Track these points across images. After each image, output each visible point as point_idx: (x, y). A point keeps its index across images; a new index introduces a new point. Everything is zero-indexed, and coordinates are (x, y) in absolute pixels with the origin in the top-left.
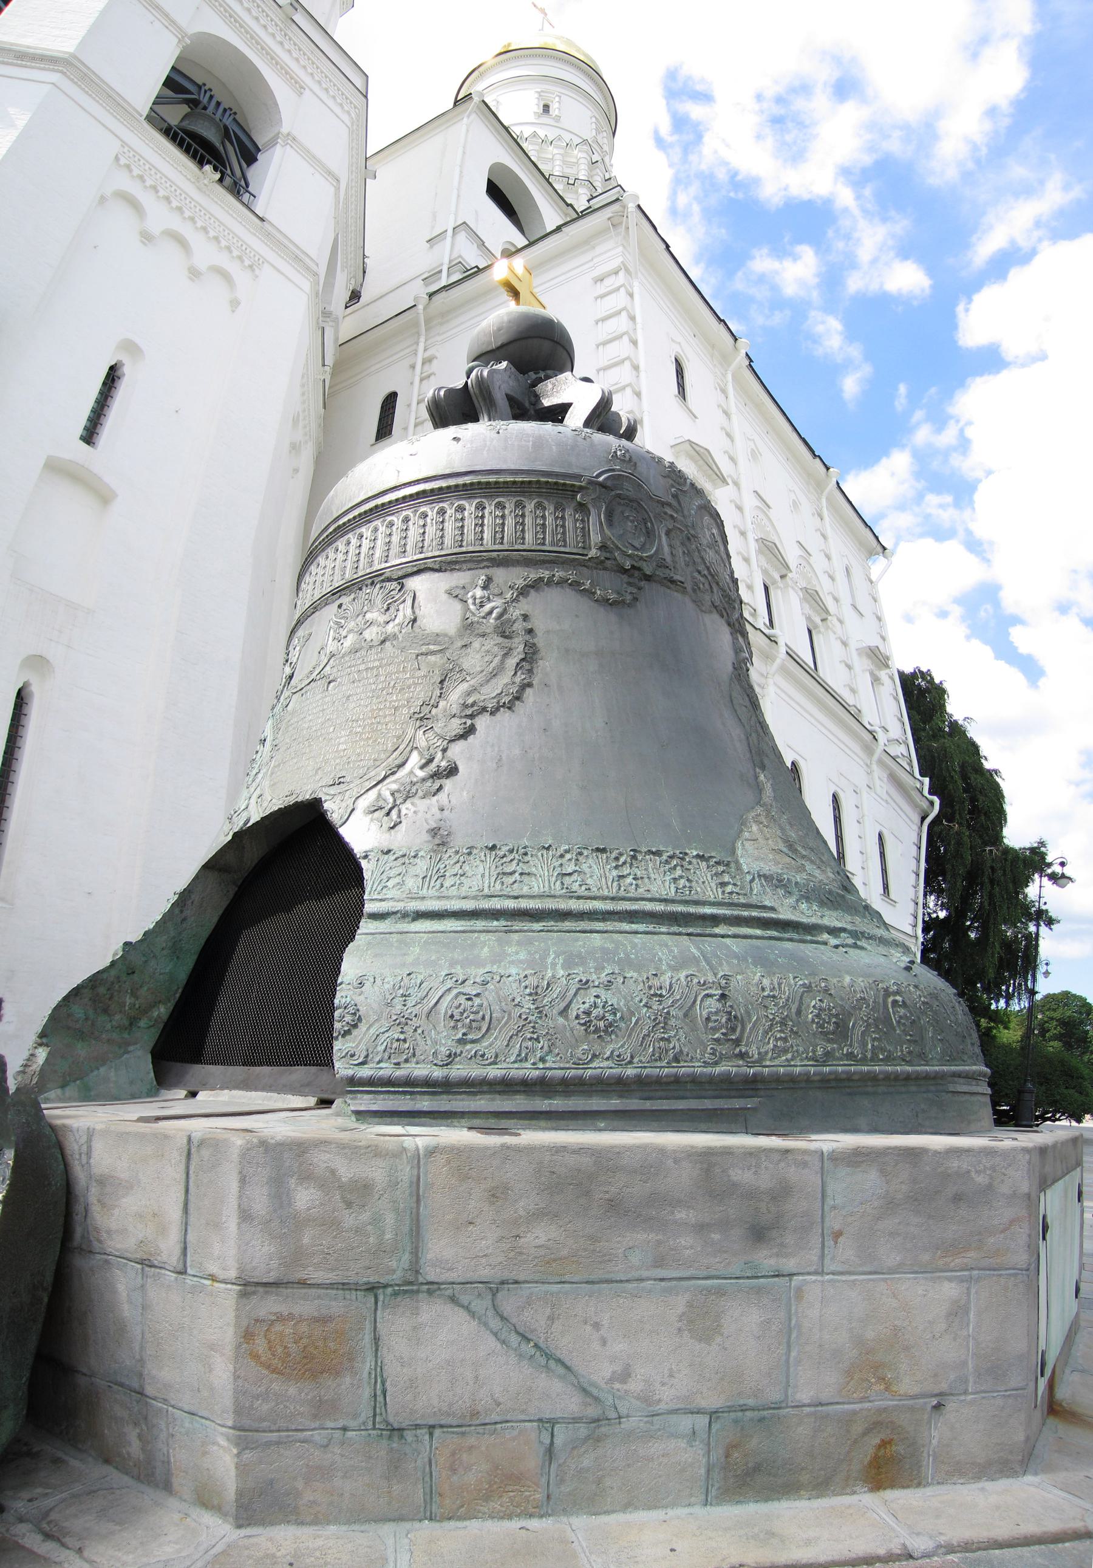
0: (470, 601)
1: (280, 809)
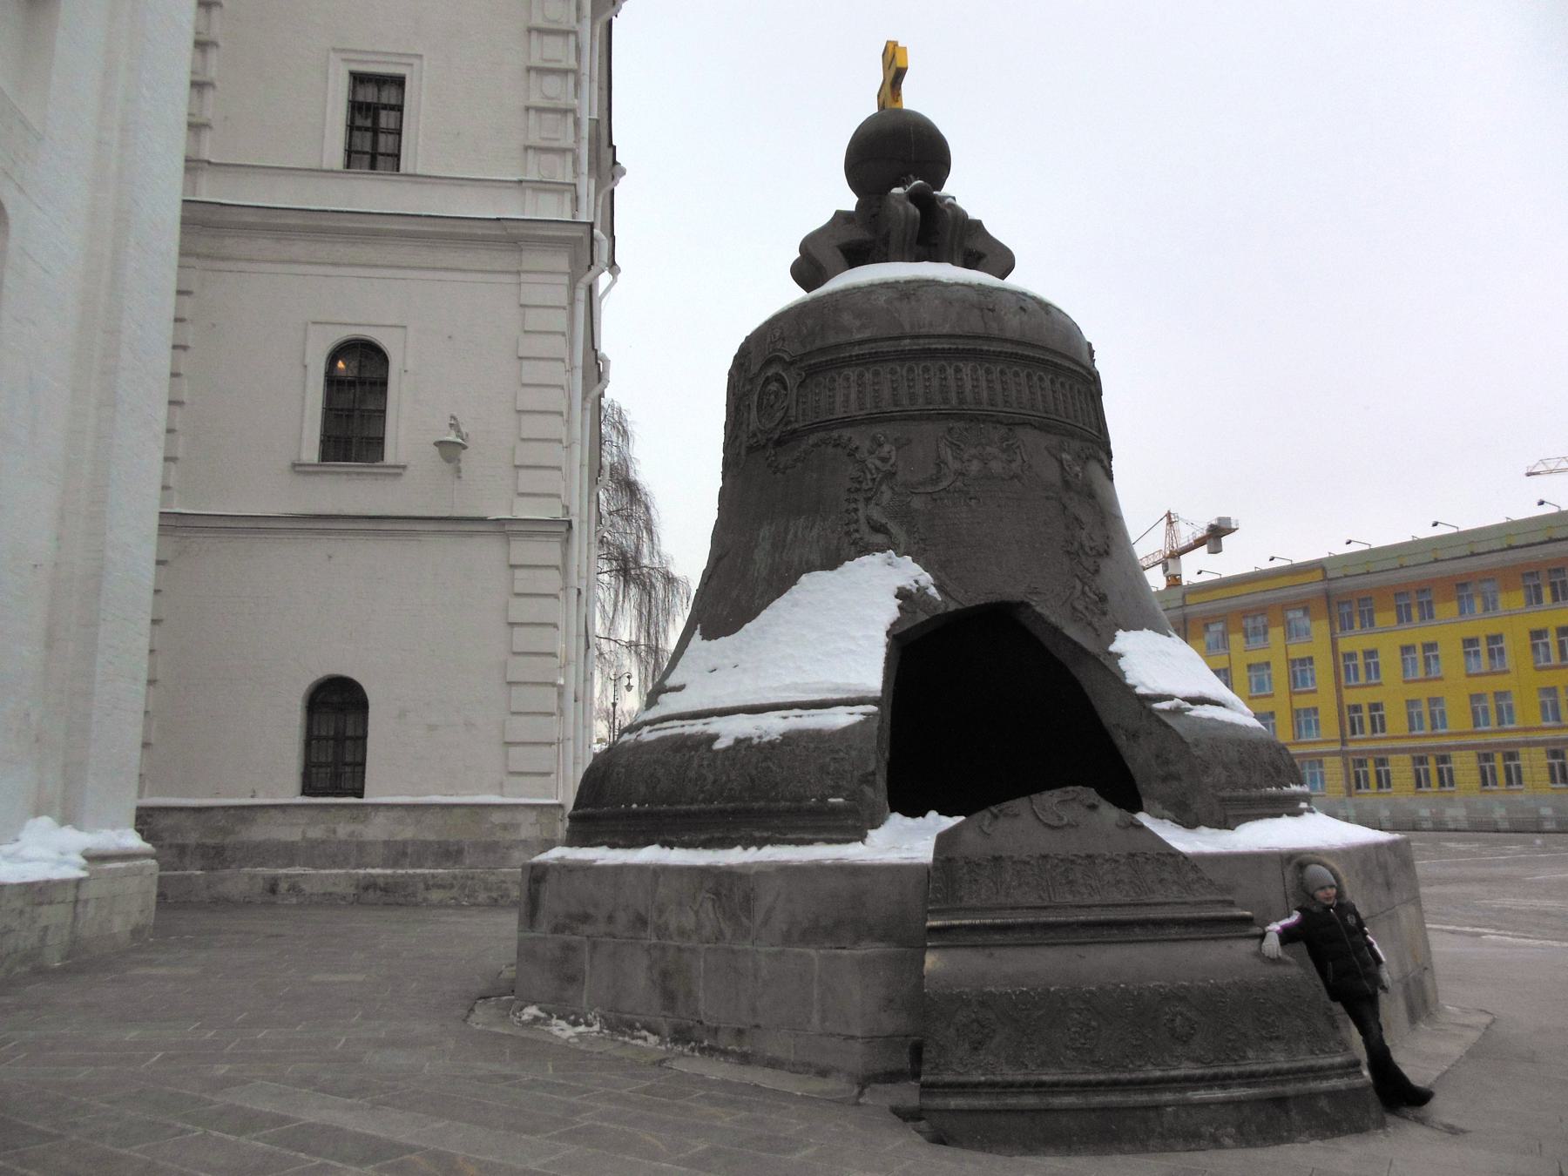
0: (1064, 462)
1: (986, 604)
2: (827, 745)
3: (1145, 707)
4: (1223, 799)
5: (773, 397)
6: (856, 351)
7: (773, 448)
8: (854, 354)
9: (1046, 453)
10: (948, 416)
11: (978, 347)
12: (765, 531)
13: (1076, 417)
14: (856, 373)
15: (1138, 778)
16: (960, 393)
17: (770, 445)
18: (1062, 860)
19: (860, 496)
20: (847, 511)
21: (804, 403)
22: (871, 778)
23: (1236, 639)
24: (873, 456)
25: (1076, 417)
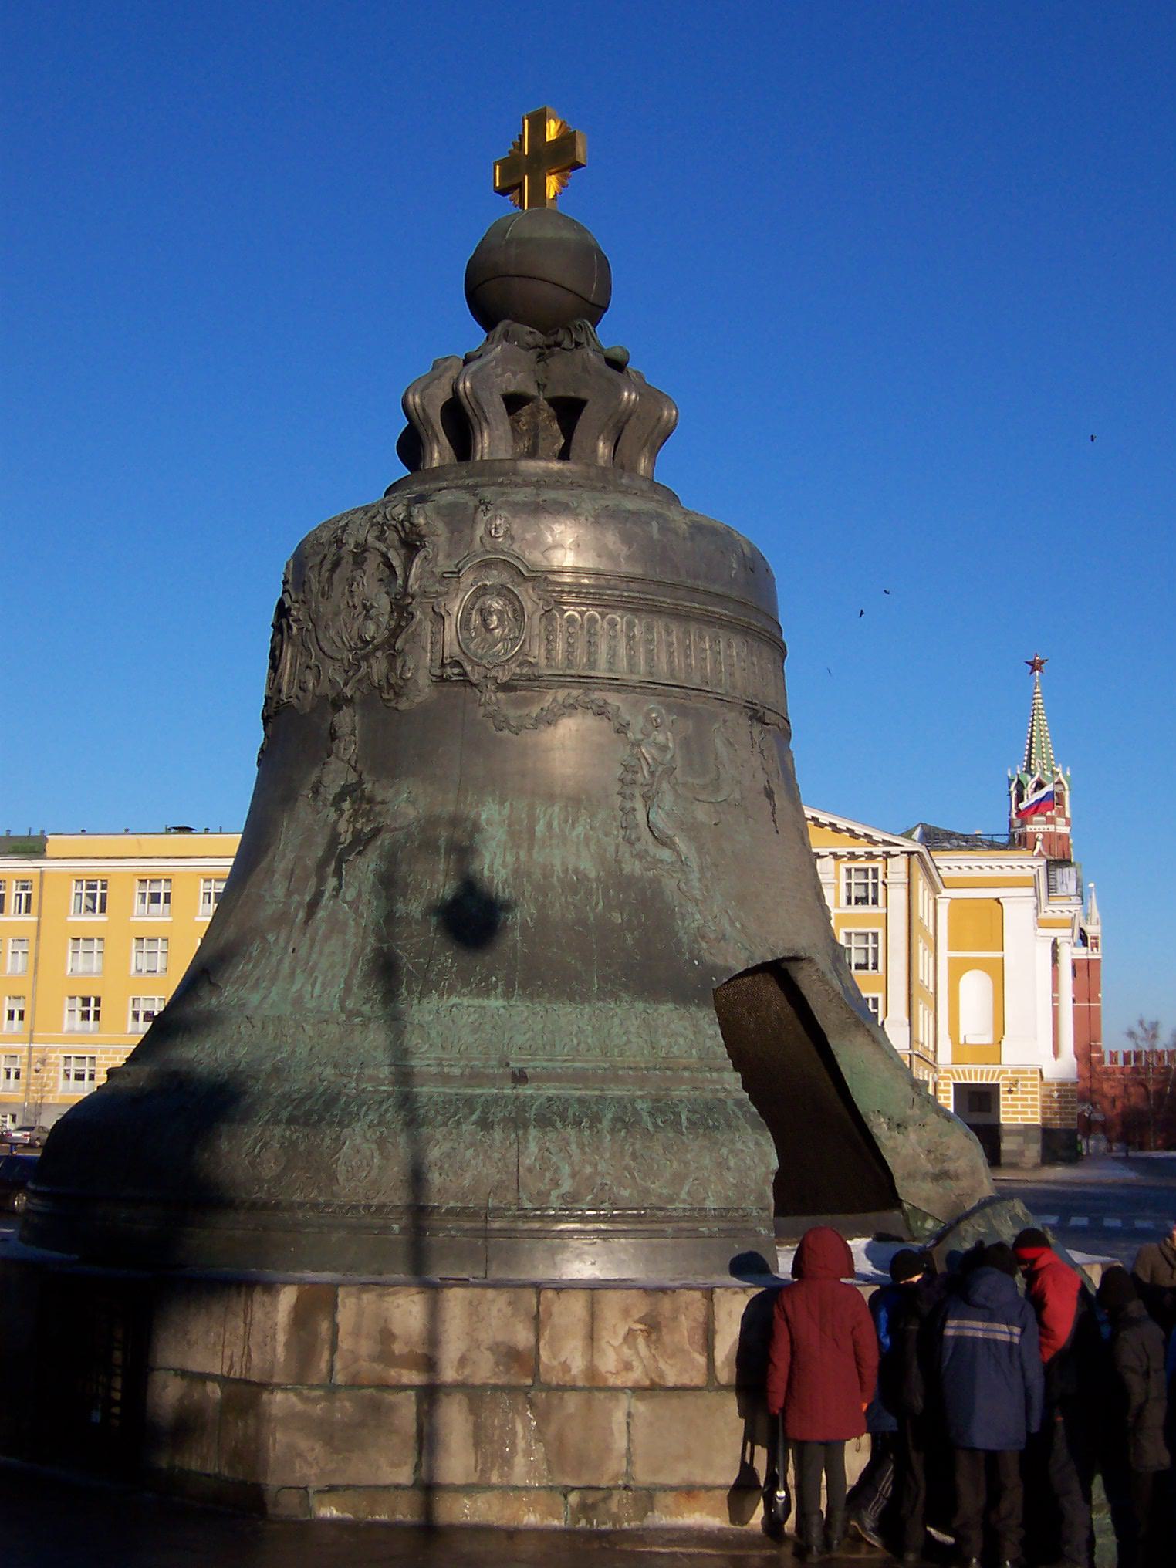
15: (897, 1175)
19: (637, 792)
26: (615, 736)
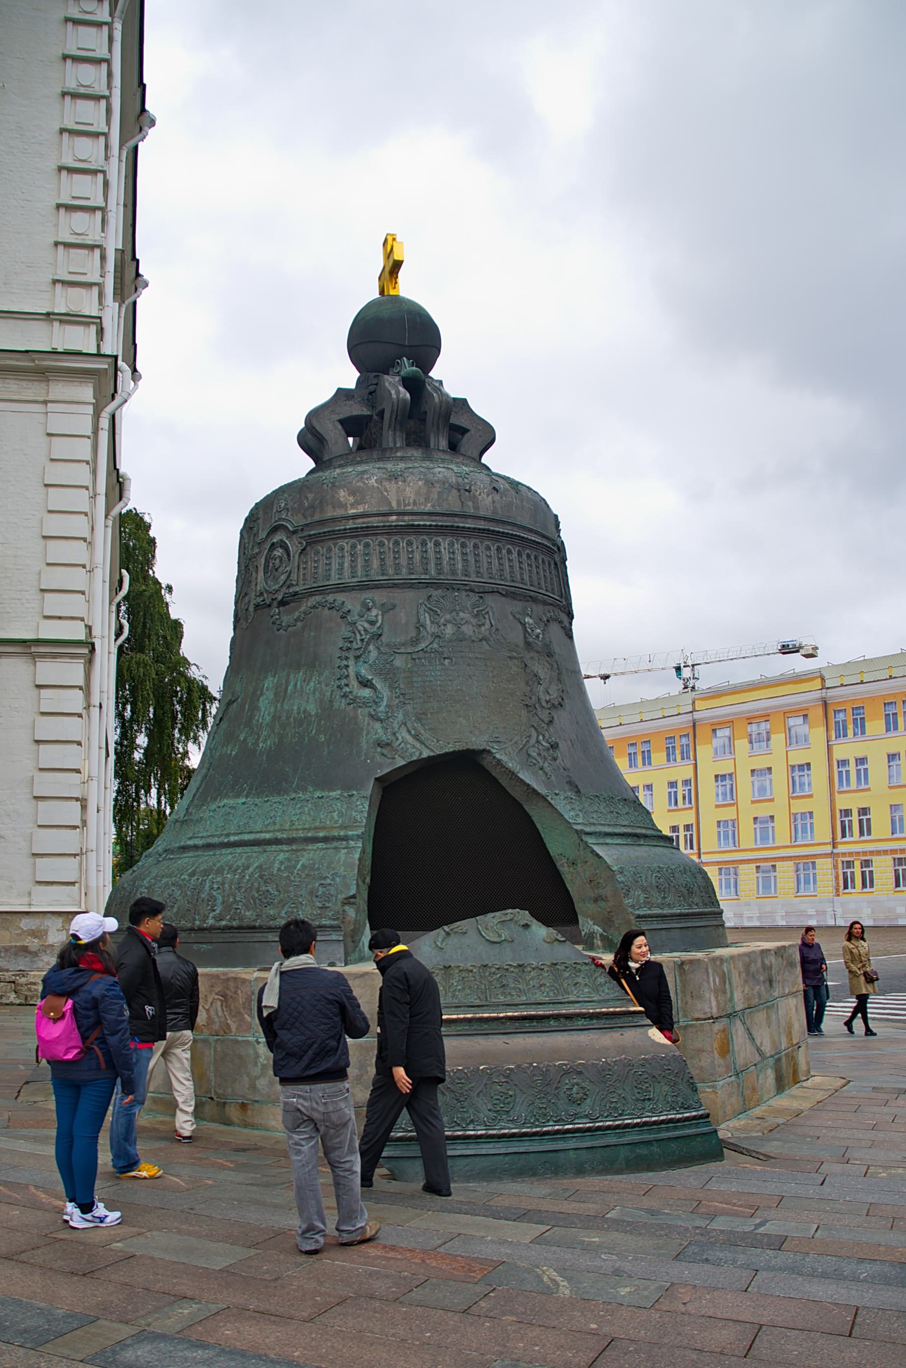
0: (527, 625)
2: (316, 873)
3: (582, 840)
4: (639, 917)
5: (278, 560)
6: (350, 525)
7: (277, 607)
8: (348, 527)
9: (511, 617)
10: (428, 585)
11: (456, 524)
12: (269, 682)
13: (539, 584)
14: (349, 545)
16: (439, 563)
17: (275, 604)
18: (498, 969)
19: (351, 655)
20: (339, 667)
21: (304, 569)
22: (352, 900)
23: (742, 745)
24: (363, 619)
25: (539, 584)
26: (339, 620)
